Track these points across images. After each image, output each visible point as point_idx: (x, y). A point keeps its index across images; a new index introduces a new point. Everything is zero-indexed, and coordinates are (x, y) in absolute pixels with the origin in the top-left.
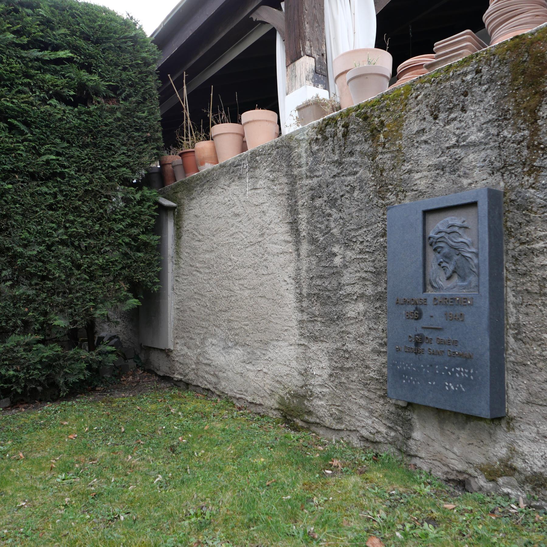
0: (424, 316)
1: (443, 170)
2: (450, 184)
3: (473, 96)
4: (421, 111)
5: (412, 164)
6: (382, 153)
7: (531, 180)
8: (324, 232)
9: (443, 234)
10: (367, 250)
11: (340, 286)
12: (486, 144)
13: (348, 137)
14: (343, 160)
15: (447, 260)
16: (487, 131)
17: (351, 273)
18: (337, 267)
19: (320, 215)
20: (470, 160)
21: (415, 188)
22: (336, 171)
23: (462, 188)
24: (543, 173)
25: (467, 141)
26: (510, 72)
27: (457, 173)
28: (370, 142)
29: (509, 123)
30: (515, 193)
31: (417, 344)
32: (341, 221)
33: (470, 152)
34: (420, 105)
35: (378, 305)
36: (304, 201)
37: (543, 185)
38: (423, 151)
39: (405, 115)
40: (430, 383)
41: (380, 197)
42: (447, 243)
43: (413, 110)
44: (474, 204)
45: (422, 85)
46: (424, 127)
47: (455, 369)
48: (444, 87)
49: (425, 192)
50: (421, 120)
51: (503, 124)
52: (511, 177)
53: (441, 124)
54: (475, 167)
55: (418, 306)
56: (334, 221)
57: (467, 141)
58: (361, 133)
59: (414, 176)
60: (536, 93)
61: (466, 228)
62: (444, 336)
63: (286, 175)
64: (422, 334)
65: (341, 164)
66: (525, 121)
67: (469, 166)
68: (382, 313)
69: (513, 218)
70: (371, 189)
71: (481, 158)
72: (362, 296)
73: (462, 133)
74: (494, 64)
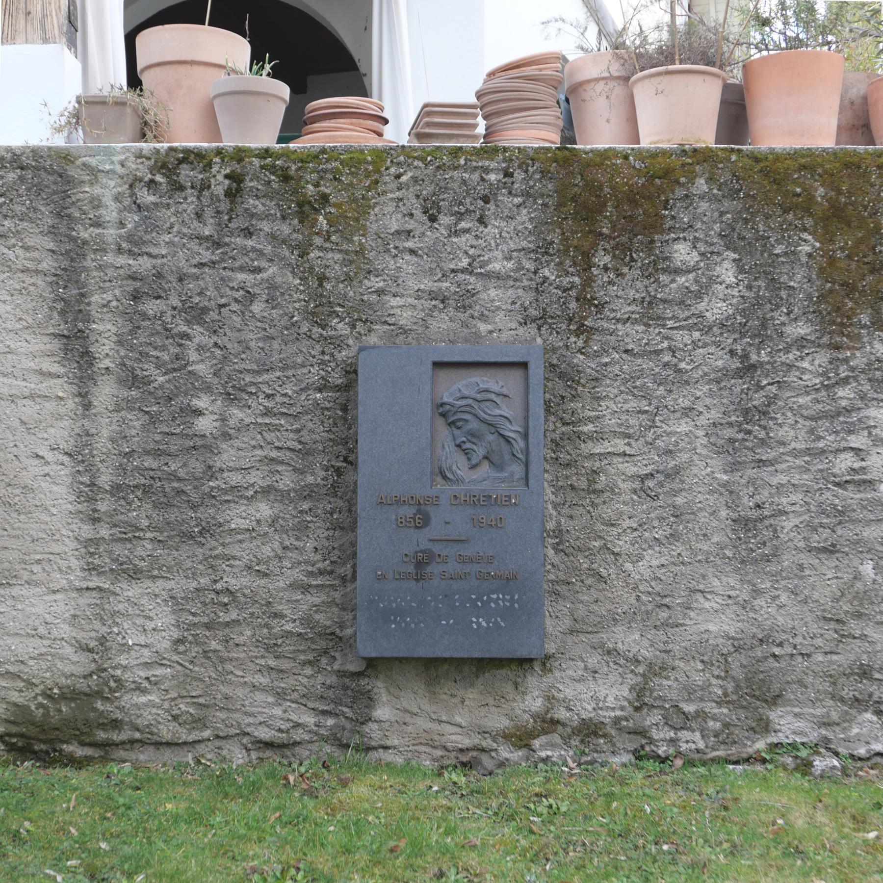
0: (433, 523)
1: (443, 302)
2: (456, 325)
3: (497, 206)
4: (405, 201)
5: (384, 280)
6: (321, 248)
7: (580, 343)
8: (169, 366)
9: (470, 402)
10: (285, 411)
11: (211, 472)
12: (516, 280)
13: (239, 199)
14: (227, 240)
15: (474, 440)
16: (519, 262)
17: (239, 449)
18: (204, 436)
19: (158, 333)
20: (491, 298)
21: (392, 320)
22: (207, 256)
23: (477, 335)
24: (595, 337)
25: (488, 268)
26: (556, 192)
27: (468, 312)
28: (296, 221)
29: (552, 260)
30: (557, 356)
31: (420, 565)
32: (218, 352)
33: (491, 285)
34: (404, 191)
35: (306, 506)
36: (108, 296)
37: (595, 351)
38: (407, 263)
39: (374, 198)
40: (443, 622)
41: (316, 322)
42: (475, 416)
43: (390, 195)
44: (524, 365)
45: (410, 161)
46: (411, 227)
47: (488, 597)
48: (451, 177)
49: (410, 330)
50: (404, 215)
51: (543, 259)
52: (551, 333)
53: (444, 232)
54: (498, 308)
55: (422, 507)
56: (197, 350)
57: (488, 268)
58: (271, 200)
59: (389, 301)
60: (590, 232)
61: (505, 396)
62: (468, 551)
63: (53, 231)
64: (430, 550)
65: (218, 244)
66: (575, 264)
67: (489, 305)
68: (314, 519)
69: (553, 389)
70: (297, 305)
71: (509, 298)
72: (267, 491)
73: (479, 256)
74: (533, 173)
